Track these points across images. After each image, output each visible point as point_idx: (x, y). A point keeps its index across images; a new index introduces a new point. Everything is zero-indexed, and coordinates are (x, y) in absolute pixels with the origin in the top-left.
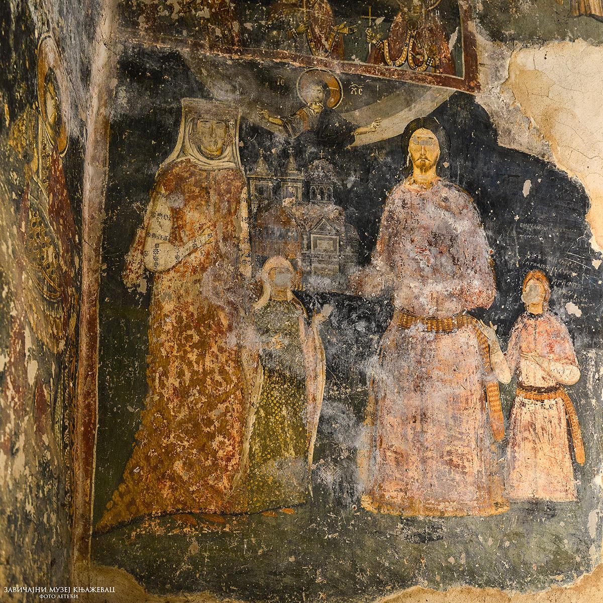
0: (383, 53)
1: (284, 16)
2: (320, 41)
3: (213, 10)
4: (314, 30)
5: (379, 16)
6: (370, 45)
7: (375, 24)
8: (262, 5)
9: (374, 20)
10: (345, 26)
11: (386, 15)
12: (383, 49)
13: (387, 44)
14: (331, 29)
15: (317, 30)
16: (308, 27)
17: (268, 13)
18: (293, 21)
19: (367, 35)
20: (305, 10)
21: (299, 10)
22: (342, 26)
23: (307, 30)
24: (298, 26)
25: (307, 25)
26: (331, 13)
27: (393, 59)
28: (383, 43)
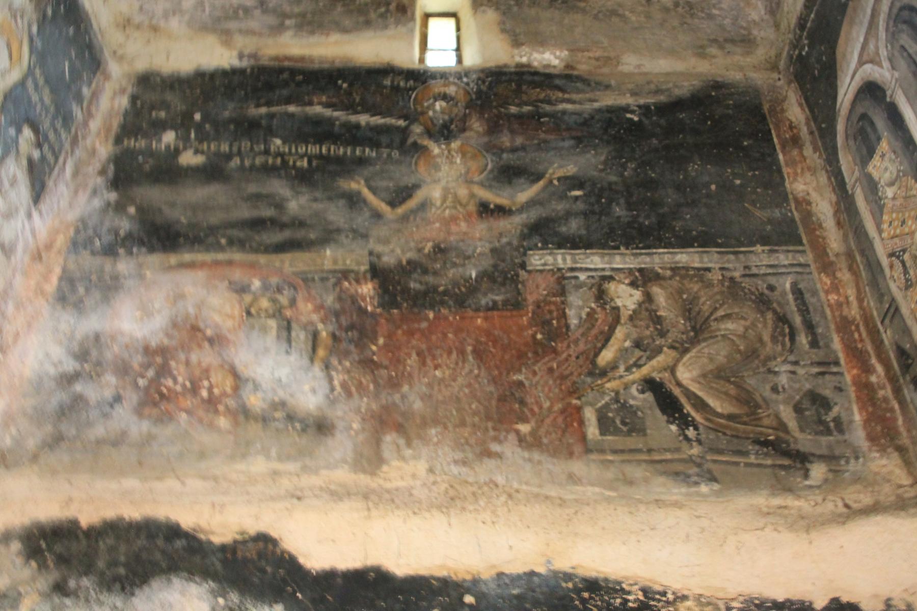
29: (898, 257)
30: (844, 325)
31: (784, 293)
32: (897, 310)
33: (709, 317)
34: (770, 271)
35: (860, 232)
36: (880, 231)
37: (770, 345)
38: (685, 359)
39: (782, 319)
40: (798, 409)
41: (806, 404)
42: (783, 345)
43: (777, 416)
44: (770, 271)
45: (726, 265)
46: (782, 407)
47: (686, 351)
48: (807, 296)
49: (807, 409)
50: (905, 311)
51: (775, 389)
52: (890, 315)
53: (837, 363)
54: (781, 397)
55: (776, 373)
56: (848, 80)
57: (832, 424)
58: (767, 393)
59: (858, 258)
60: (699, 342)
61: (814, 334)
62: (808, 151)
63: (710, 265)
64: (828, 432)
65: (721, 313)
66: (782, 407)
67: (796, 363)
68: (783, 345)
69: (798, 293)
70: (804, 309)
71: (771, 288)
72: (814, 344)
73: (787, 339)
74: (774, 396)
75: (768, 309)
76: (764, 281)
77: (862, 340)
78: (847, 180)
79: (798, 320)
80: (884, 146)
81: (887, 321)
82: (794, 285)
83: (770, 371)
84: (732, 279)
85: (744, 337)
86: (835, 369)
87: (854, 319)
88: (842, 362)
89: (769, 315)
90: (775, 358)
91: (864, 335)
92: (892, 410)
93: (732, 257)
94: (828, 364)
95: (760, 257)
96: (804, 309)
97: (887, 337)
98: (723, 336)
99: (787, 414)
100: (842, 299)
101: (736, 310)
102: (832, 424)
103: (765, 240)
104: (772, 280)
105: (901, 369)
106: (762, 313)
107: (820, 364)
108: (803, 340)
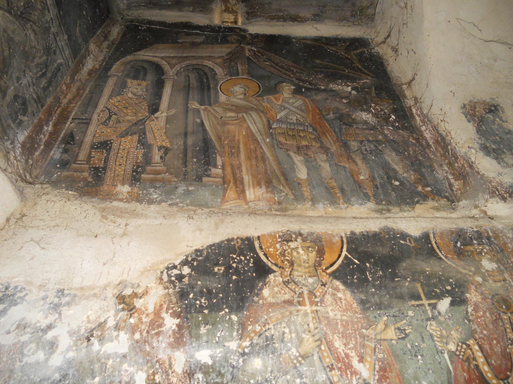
0: (477, 366)
1: (271, 326)
2: (349, 366)
3: (137, 336)
4: (333, 344)
5: (439, 297)
6: (446, 356)
7: (439, 313)
8: (230, 312)
9: (434, 306)
10: (386, 326)
11: (450, 293)
12: (474, 359)
13: (477, 347)
14: (363, 336)
15: (338, 344)
16: (319, 340)
17: (243, 326)
18: (290, 332)
19: (432, 336)
20: (308, 308)
21: (298, 311)
22: (381, 326)
23: (319, 346)
24: (301, 341)
25: (317, 337)
26: (355, 305)
27: (502, 376)
28: (468, 346)
29: (110, 113)
30: (57, 100)
31: (55, 61)
32: (88, 124)
33: (30, 21)
34: (61, 47)
35: (98, 89)
36: (110, 97)
37: (34, 64)
38: (6, 14)
39: (46, 65)
40: (16, 97)
41: (20, 101)
42: (37, 73)
43: (8, 88)
44: (61, 47)
45: (54, 21)
46: (12, 88)
47: (10, 13)
48: (59, 74)
49: (18, 102)
50: (92, 129)
51: (18, 79)
52: (81, 121)
53: (42, 106)
54: (17, 85)
55: (25, 75)
56: (151, 54)
57: (18, 120)
58: (14, 76)
59: (87, 92)
60: (17, 19)
61: (48, 87)
62: (105, 44)
63: (51, 11)
64: (14, 121)
65: (35, 28)
66: (12, 88)
67: (34, 85)
68: (37, 73)
69: (58, 69)
70: (54, 75)
71: (55, 53)
72: (45, 89)
73: (40, 73)
74: (15, 81)
75: (47, 55)
76: (56, 47)
77: (55, 112)
78: (112, 70)
79: (49, 75)
80: (144, 83)
81: (77, 121)
82: (60, 65)
83: (24, 71)
84: (50, 27)
85: (31, 47)
86: (40, 106)
87: (61, 103)
88: (44, 108)
89: (45, 58)
90: (30, 71)
91: (58, 112)
92: (39, 146)
93: (58, 23)
94: (40, 102)
95: (63, 40)
96: (54, 75)
97: (69, 125)
98: (26, 34)
99: (11, 92)
100: (65, 92)
101: (39, 37)
102: (18, 120)
103: (69, 38)
104: (58, 52)
105: (63, 139)
106: (44, 53)
107: (38, 97)
108: (44, 82)
